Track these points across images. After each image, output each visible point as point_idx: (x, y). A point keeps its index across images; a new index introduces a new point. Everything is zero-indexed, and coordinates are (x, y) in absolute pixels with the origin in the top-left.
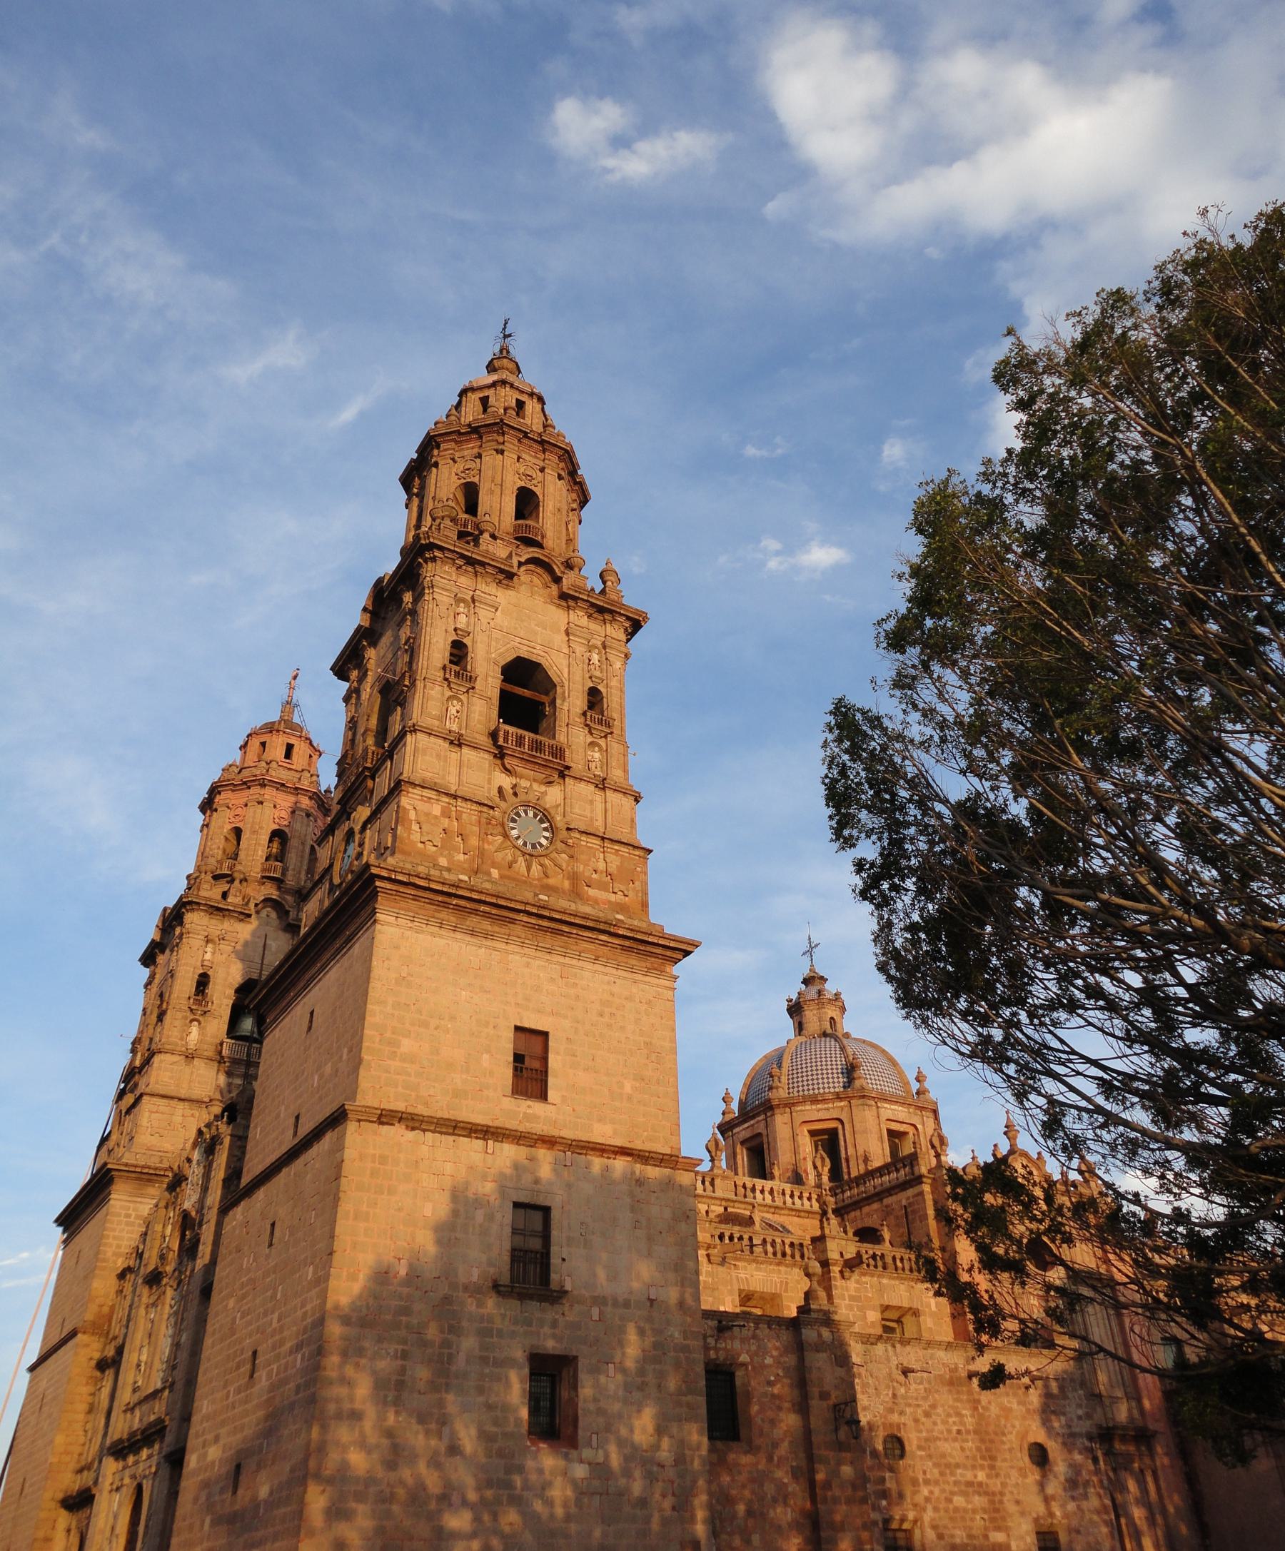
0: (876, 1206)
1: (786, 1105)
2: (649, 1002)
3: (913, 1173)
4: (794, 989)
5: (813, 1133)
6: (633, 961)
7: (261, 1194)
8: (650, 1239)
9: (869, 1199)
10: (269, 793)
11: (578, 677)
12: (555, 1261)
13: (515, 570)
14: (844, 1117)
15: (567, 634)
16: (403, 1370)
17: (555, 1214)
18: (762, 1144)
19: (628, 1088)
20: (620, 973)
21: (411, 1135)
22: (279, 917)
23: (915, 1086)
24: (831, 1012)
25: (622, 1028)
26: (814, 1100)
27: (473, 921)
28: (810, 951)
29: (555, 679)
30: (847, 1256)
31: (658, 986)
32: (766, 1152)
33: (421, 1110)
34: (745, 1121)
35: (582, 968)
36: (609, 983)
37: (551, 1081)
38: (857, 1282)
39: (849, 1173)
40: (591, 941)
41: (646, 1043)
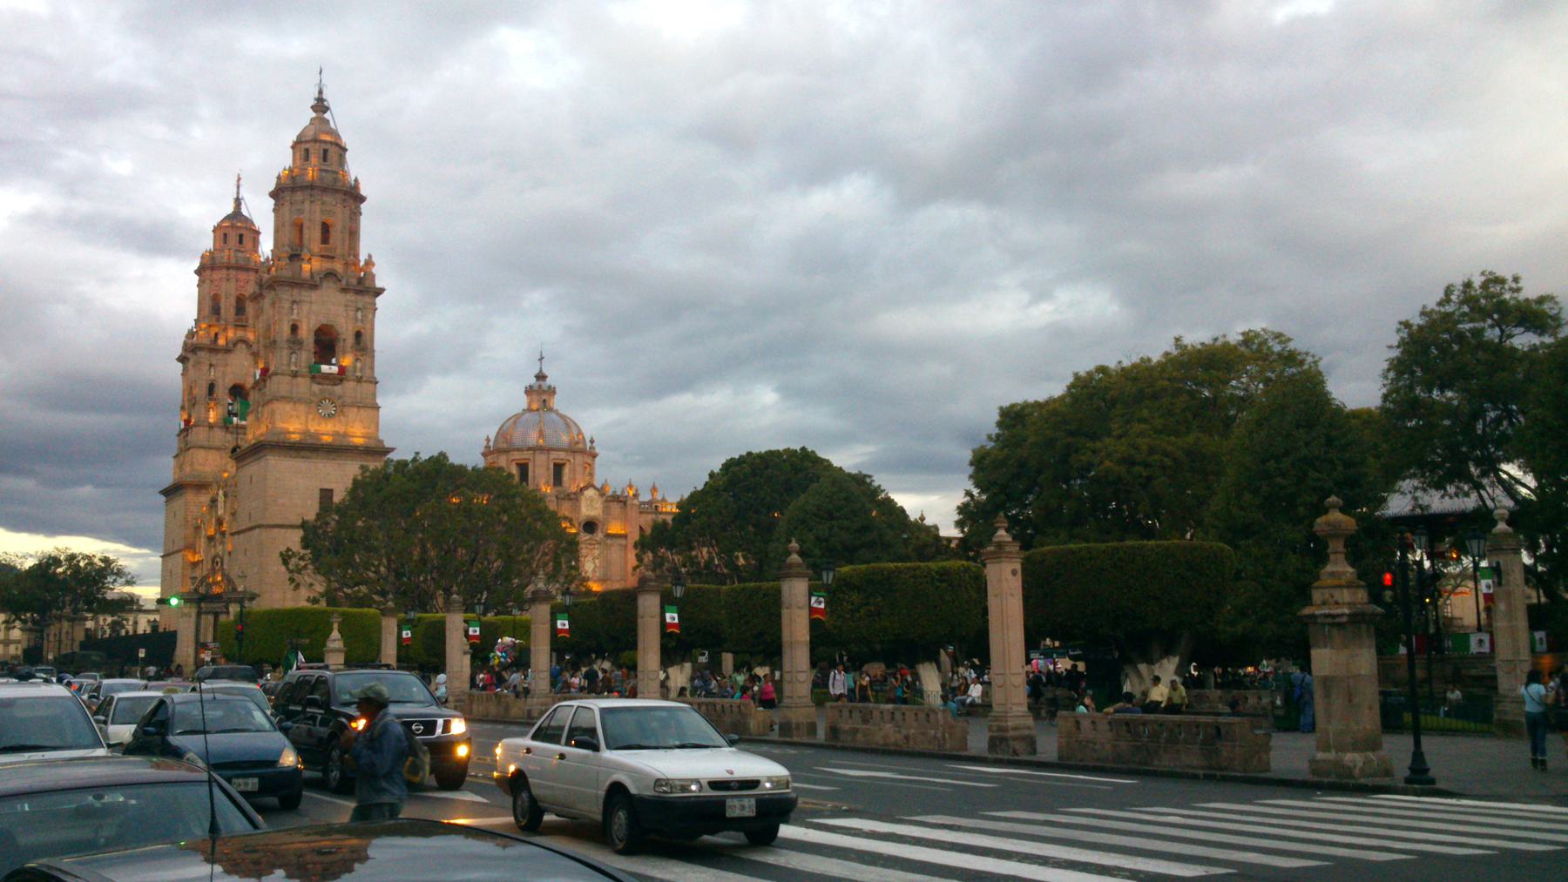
5: (517, 464)
7: (241, 536)
10: (233, 273)
11: (350, 328)
13: (318, 283)
14: (531, 458)
15: (346, 306)
16: (284, 597)
21: (283, 530)
22: (247, 347)
24: (544, 397)
26: (518, 450)
27: (302, 453)
28: (541, 359)
29: (340, 332)
33: (287, 523)
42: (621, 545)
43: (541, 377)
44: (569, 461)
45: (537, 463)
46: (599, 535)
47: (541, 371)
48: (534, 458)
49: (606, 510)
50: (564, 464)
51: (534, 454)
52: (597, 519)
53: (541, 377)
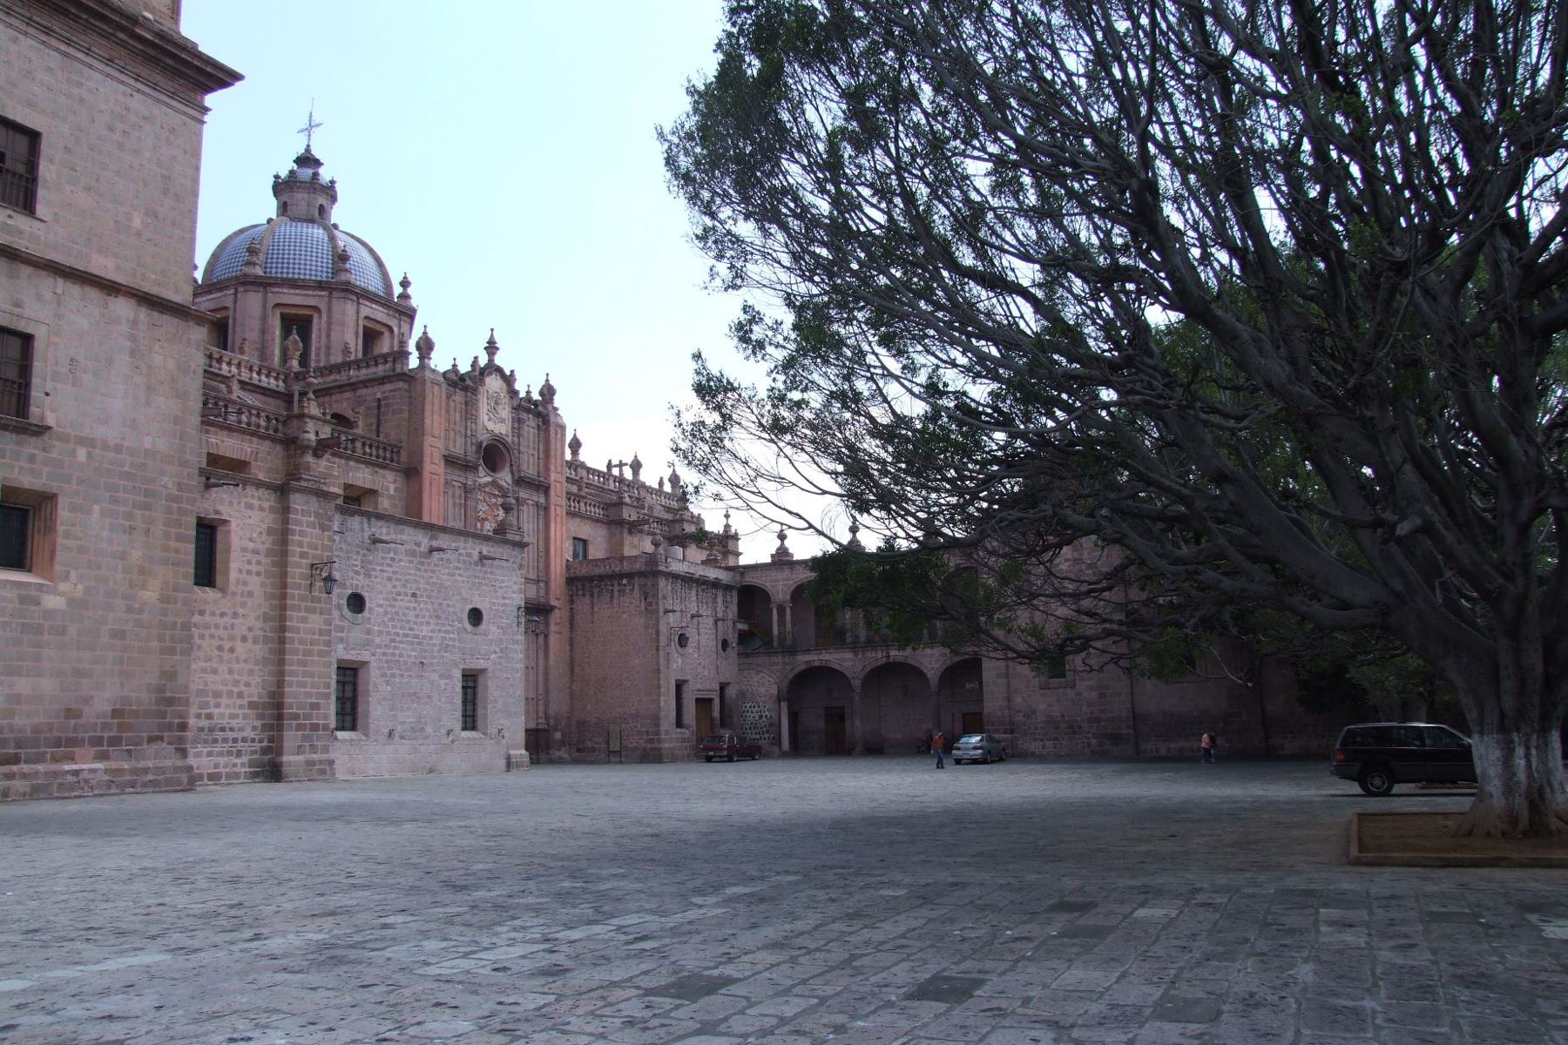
0: (348, 395)
1: (261, 284)
2: (173, 130)
3: (394, 370)
4: (285, 167)
5: (284, 318)
6: (158, 78)
8: (150, 388)
9: (341, 388)
12: (36, 394)
14: (323, 306)
17: (39, 346)
18: (227, 318)
19: (137, 222)
20: (139, 85)
23: (397, 290)
24: (321, 200)
25: (137, 152)
28: (310, 127)
30: (322, 436)
31: (185, 114)
32: (230, 331)
34: (210, 292)
35: (90, 67)
36: (124, 94)
37: (41, 193)
38: (329, 461)
39: (318, 361)
40: (106, 36)
41: (163, 176)
42: (537, 504)
43: (307, 160)
44: (391, 329)
45: (336, 316)
46: (505, 478)
47: (308, 149)
48: (329, 310)
49: (518, 422)
50: (382, 333)
51: (330, 296)
52: (504, 444)
53: (307, 160)
